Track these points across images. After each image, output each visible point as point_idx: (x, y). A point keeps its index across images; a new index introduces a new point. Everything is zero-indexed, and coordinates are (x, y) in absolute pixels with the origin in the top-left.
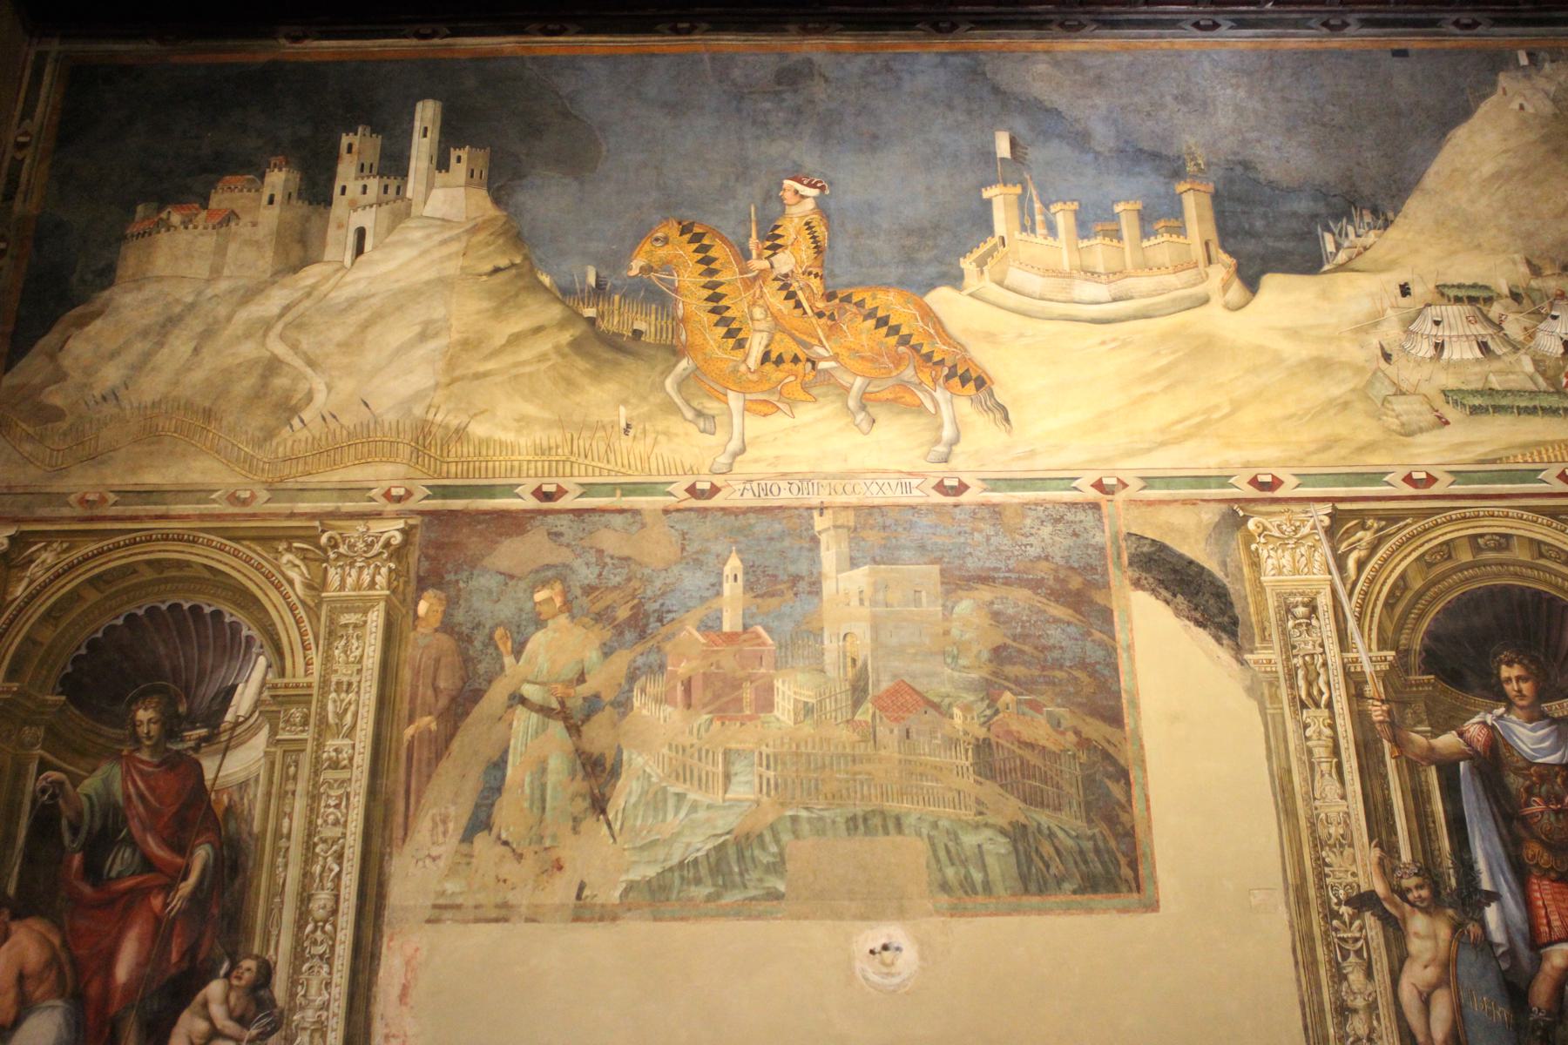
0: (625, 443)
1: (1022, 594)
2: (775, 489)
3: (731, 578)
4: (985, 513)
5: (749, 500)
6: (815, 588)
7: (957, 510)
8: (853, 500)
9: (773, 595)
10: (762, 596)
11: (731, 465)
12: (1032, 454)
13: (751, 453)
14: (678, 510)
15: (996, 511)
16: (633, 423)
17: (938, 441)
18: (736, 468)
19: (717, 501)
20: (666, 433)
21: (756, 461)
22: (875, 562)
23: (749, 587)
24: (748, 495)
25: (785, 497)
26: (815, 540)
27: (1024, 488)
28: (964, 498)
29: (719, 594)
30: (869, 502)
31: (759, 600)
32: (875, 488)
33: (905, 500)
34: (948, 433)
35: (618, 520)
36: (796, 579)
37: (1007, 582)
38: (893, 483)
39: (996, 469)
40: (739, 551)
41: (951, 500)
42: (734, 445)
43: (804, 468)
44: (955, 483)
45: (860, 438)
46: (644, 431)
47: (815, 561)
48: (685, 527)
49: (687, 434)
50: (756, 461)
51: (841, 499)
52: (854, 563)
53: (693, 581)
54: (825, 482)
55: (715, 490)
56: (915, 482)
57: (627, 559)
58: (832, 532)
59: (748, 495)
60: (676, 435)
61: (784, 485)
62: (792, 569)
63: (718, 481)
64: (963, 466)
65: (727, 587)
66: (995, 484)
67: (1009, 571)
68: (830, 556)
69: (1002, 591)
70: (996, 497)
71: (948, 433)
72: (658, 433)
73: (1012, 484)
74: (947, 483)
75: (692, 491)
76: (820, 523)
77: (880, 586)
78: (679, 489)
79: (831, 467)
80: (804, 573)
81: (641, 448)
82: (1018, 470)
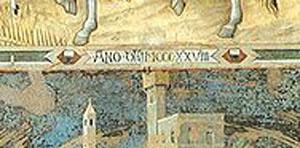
0: (15, 20)
1: (277, 135)
2: (117, 57)
3: (88, 123)
4: (255, 76)
5: (99, 65)
6: (143, 130)
7: (238, 73)
8: (169, 64)
9: (115, 135)
10: (109, 136)
11: (88, 38)
12: (291, 31)
13: (101, 29)
14: (53, 72)
15: (263, 74)
16: (20, 5)
17: (228, 21)
18: (91, 42)
19: (78, 66)
20: (43, 14)
21: (104, 35)
22: (183, 111)
23: (101, 127)
24: (99, 60)
25: (123, 63)
26: (143, 94)
27: (284, 57)
28: (242, 64)
29: (80, 133)
30: (180, 67)
31: (106, 138)
32: (184, 57)
33: (204, 65)
34: (234, 14)
35: (12, 79)
36: (131, 122)
37: (268, 126)
38: (196, 53)
39: (263, 44)
40: (94, 103)
41: (235, 66)
42: (89, 23)
43: (136, 41)
44: (237, 53)
45: (174, 18)
46: (28, 11)
47: (143, 110)
48: (58, 85)
49: (57, 14)
50: (104, 35)
51: (161, 64)
52: (168, 113)
53: (64, 124)
54: (150, 52)
55: (77, 57)
56: (211, 52)
57: (19, 108)
58: (155, 88)
59: (99, 60)
60: (51, 15)
61: (123, 53)
62: (127, 116)
63: (79, 50)
64: (245, 41)
65: (85, 128)
66: (263, 54)
67: (270, 118)
68: (151, 106)
69: (264, 132)
70: (264, 64)
71: (234, 14)
72: (38, 13)
73: (275, 54)
74: (232, 53)
75: (61, 57)
76: (147, 81)
77: (186, 129)
78: (53, 56)
79: (154, 41)
80: (136, 119)
81: (26, 24)
82: (281, 44)
